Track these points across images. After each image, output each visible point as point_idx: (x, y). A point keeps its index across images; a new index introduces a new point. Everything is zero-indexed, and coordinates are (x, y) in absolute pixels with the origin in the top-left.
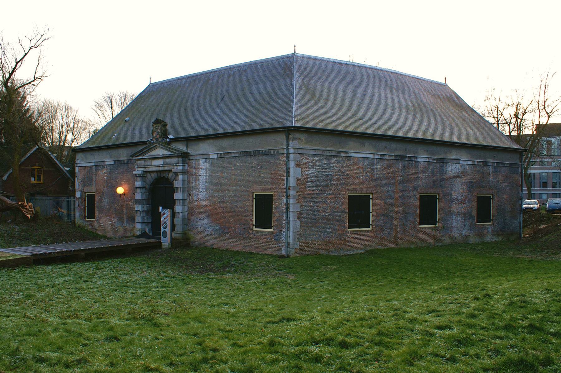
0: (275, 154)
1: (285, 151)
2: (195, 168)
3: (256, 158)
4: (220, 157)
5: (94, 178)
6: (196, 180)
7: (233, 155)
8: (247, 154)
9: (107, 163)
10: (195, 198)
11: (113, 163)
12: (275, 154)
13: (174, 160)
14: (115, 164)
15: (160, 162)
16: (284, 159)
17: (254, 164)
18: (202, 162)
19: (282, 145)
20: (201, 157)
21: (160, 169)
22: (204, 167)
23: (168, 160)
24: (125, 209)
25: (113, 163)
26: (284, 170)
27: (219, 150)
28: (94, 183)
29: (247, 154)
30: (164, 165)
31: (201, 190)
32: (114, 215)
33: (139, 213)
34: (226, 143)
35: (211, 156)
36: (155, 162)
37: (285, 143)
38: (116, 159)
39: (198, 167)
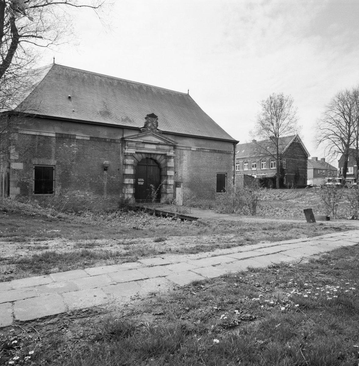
0: (229, 153)
1: (233, 153)
2: (180, 155)
3: (219, 154)
4: (198, 150)
5: (53, 150)
6: (181, 163)
7: (206, 151)
8: (215, 151)
9: (77, 137)
10: (179, 175)
11: (89, 139)
12: (229, 153)
13: (167, 147)
14: (90, 140)
15: (154, 147)
16: (232, 157)
17: (218, 157)
18: (185, 152)
19: (231, 149)
20: (185, 148)
21: (154, 152)
22: (186, 156)
23: (160, 146)
24: (105, 183)
25: (89, 139)
26: (232, 163)
27: (197, 146)
28: (53, 155)
29: (215, 151)
30: (157, 149)
31: (184, 169)
32: (89, 188)
33: (130, 185)
34: (202, 142)
35: (192, 149)
36: (147, 146)
37: (233, 149)
38: (92, 136)
39: (182, 155)
